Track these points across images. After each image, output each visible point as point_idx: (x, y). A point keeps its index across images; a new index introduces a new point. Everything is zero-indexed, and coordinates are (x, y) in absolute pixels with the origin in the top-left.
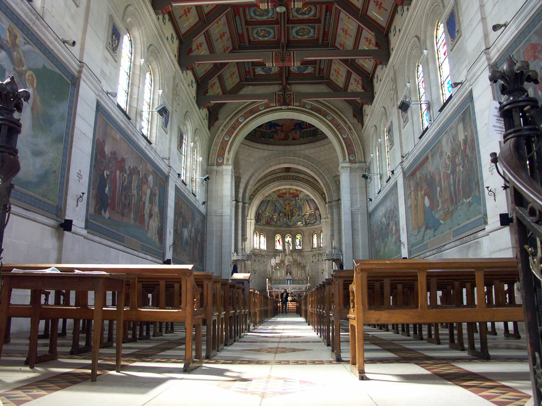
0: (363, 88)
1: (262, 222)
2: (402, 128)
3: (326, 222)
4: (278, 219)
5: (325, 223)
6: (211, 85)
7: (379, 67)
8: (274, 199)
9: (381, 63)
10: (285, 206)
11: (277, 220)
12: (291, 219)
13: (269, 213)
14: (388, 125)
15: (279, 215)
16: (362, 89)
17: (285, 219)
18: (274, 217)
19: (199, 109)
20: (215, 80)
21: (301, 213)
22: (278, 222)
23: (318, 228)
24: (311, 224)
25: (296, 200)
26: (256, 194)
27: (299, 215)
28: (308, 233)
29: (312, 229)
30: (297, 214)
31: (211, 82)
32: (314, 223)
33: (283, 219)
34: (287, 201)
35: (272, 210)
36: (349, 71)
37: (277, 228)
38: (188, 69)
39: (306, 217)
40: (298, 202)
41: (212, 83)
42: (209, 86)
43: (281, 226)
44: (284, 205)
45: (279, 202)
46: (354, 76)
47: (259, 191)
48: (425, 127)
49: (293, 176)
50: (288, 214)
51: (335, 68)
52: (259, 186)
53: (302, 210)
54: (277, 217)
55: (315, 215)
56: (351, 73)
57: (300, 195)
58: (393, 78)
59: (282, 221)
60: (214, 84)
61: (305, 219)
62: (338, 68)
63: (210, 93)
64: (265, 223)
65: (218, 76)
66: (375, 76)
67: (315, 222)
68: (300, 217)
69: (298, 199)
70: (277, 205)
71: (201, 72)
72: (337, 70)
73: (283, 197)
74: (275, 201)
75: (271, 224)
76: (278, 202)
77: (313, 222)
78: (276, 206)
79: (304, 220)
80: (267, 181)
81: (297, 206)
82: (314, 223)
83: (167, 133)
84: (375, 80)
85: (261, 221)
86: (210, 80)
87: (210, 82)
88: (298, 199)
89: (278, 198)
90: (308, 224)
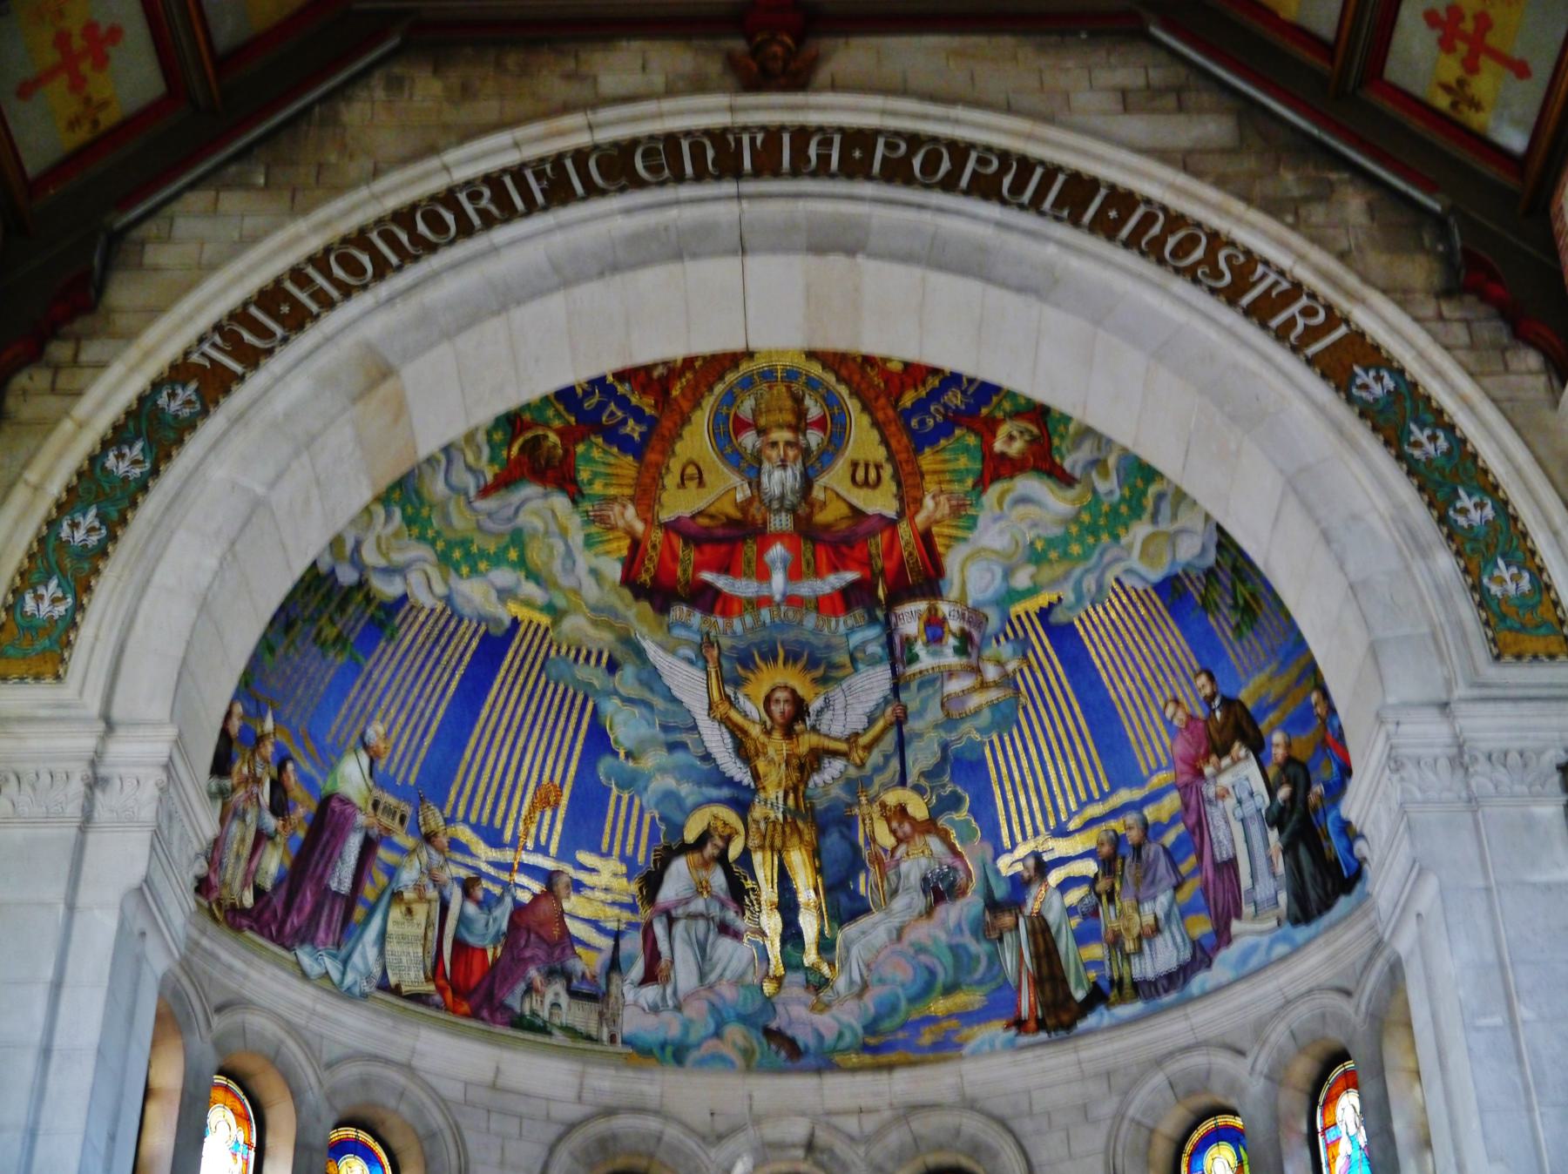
1: (366, 952)
3: (1460, 758)
4: (633, 944)
5: (1441, 782)
8: (576, 625)
10: (743, 749)
11: (615, 965)
12: (825, 946)
13: (493, 837)
15: (652, 882)
17: (731, 955)
18: (571, 903)
21: (973, 855)
22: (633, 997)
23: (1259, 1029)
24: (1143, 989)
25: (897, 653)
26: (253, 359)
27: (940, 890)
28: (1094, 1140)
29: (1158, 1062)
30: (916, 864)
32: (1176, 978)
33: (702, 948)
34: (774, 677)
35: (545, 800)
37: (607, 1082)
39: (1048, 901)
40: (930, 680)
43: (677, 1053)
44: (717, 742)
45: (651, 678)
47: (298, 321)
49: (857, 140)
50: (784, 880)
52: (319, 261)
53: (983, 808)
54: (613, 918)
55: (1198, 830)
57: (953, 562)
59: (685, 974)
61: (1041, 932)
64: (412, 976)
67: (1202, 956)
68: (954, 913)
69: (934, 627)
70: (626, 726)
73: (707, 599)
74: (580, 654)
75: (514, 1000)
76: (627, 678)
77: (1164, 956)
78: (599, 740)
79: (1016, 956)
80: (448, 197)
81: (922, 757)
82: (1176, 978)
85: (347, 930)
88: (934, 627)
89: (636, 615)
90: (1097, 997)
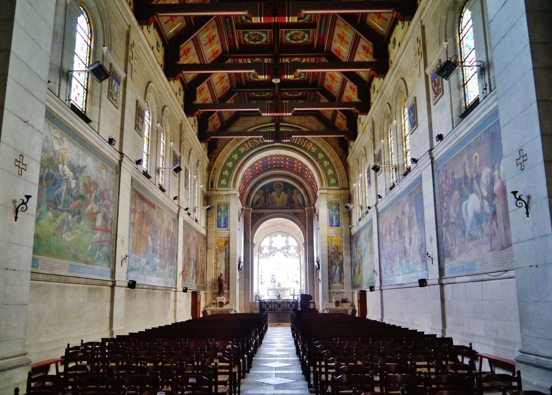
0: (375, 55)
2: (432, 103)
6: (184, 51)
7: (399, 28)
9: (403, 20)
14: (410, 101)
16: (374, 58)
19: (169, 80)
20: (189, 44)
31: (183, 47)
36: (357, 35)
38: (148, 24)
41: (186, 48)
42: (182, 53)
46: (363, 42)
48: (470, 100)
51: (339, 32)
56: (360, 37)
58: (420, 38)
60: (189, 50)
62: (343, 32)
63: (183, 61)
65: (193, 39)
66: (392, 40)
71: (170, 31)
72: (342, 35)
83: (117, 108)
84: (391, 46)
86: (182, 44)
87: (181, 46)
